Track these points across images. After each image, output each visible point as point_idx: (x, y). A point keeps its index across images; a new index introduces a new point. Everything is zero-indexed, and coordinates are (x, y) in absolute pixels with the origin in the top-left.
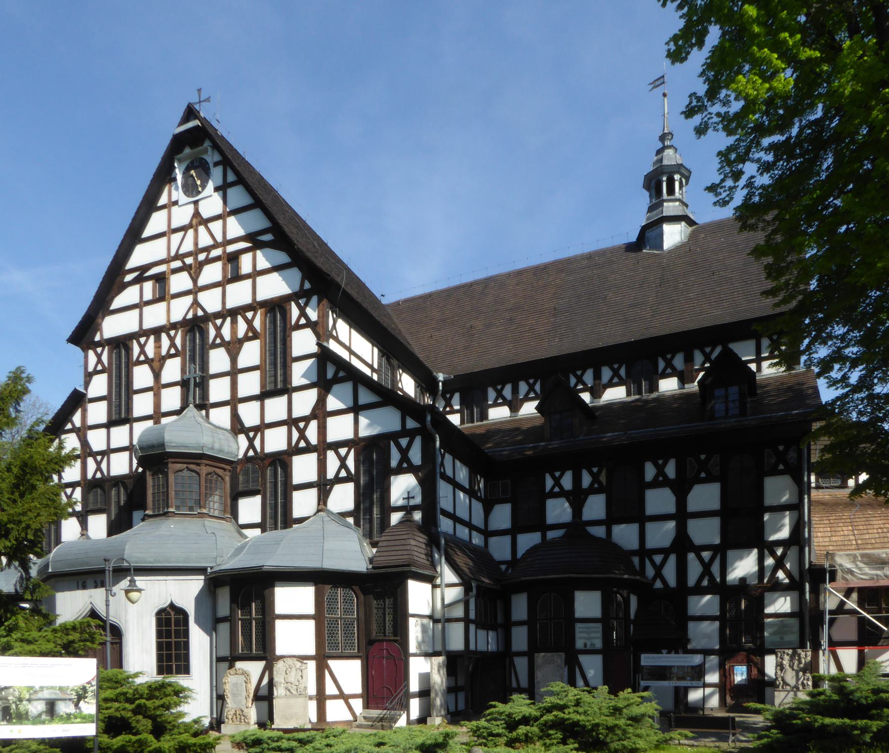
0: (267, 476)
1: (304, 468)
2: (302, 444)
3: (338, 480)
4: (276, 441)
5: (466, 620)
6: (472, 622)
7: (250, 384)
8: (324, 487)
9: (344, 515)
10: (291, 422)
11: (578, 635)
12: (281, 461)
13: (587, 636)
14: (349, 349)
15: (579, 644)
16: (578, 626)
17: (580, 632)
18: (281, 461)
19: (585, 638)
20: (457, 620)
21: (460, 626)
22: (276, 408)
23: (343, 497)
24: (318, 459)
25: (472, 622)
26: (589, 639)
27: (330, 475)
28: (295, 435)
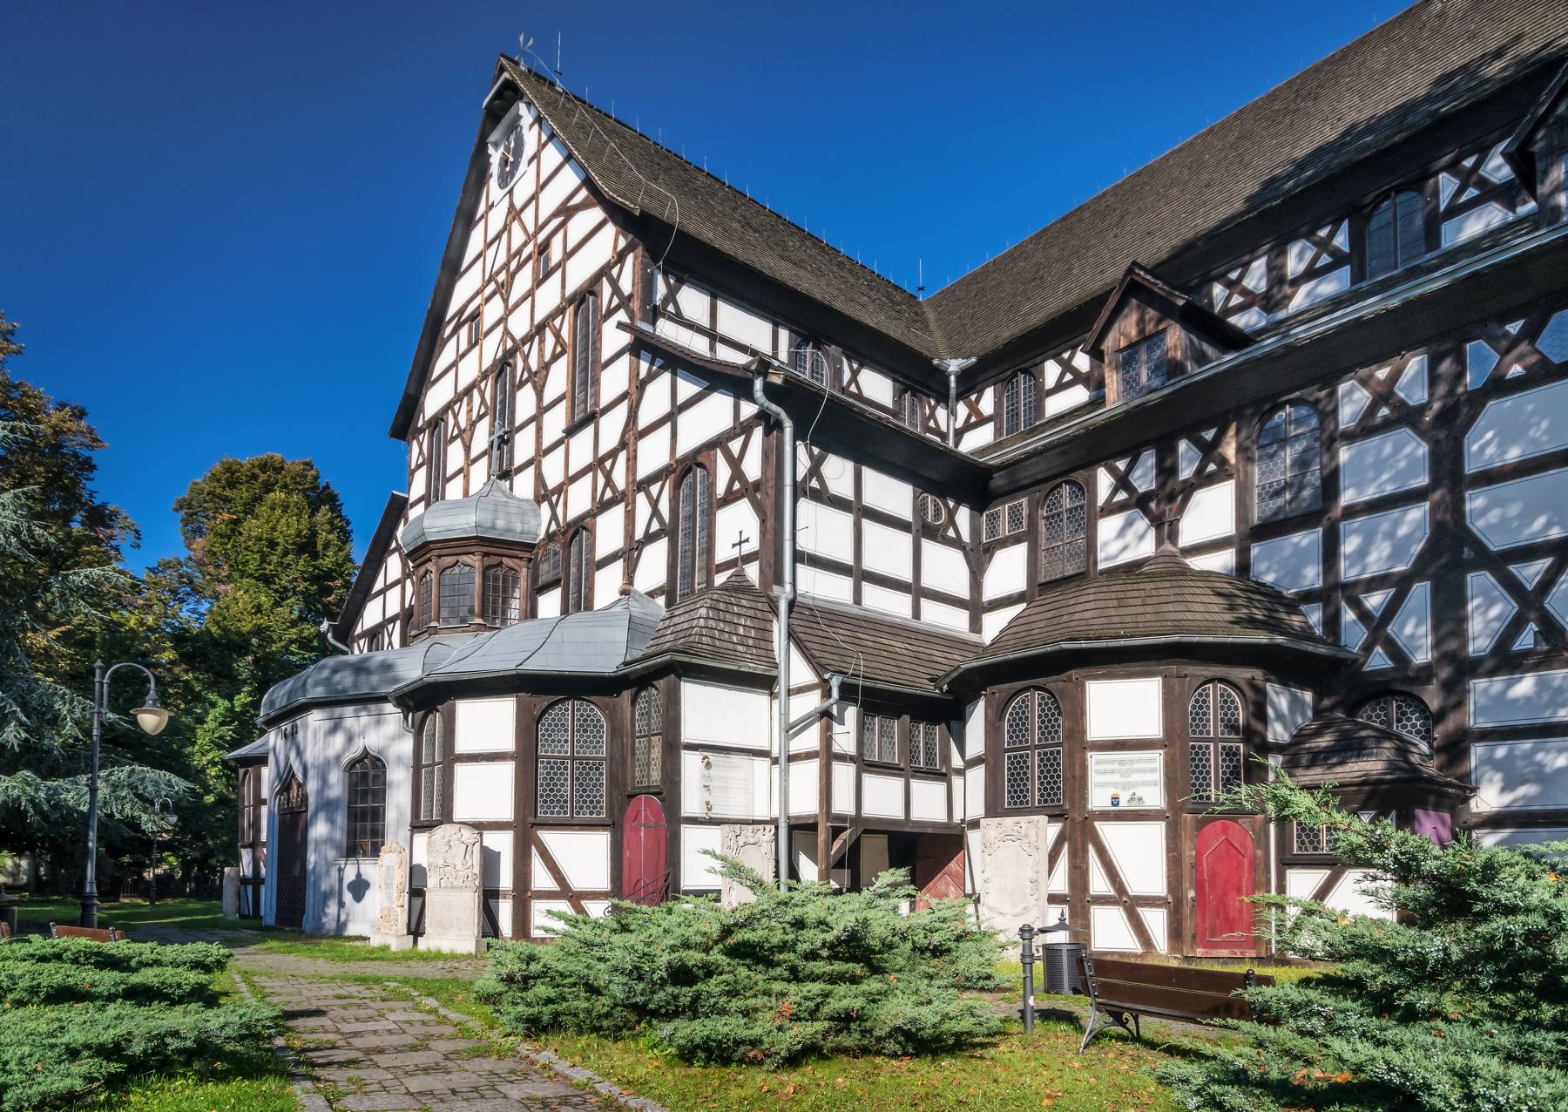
0: (563, 559)
1: (609, 533)
2: (609, 494)
3: (650, 538)
4: (579, 500)
5: (828, 756)
6: (843, 758)
7: (556, 422)
8: (630, 554)
9: (652, 594)
10: (599, 464)
11: (1093, 778)
12: (581, 528)
13: (1125, 781)
14: (713, 336)
15: (1098, 799)
16: (1094, 759)
17: (1097, 772)
18: (581, 528)
19: (1115, 785)
20: (809, 756)
21: (814, 766)
22: (582, 449)
23: (654, 566)
24: (627, 512)
25: (843, 758)
26: (1125, 787)
27: (639, 534)
28: (601, 481)
